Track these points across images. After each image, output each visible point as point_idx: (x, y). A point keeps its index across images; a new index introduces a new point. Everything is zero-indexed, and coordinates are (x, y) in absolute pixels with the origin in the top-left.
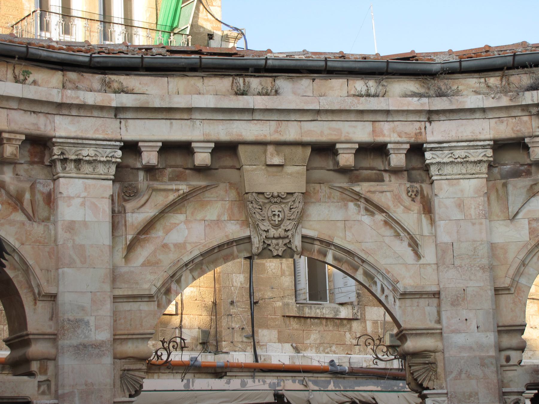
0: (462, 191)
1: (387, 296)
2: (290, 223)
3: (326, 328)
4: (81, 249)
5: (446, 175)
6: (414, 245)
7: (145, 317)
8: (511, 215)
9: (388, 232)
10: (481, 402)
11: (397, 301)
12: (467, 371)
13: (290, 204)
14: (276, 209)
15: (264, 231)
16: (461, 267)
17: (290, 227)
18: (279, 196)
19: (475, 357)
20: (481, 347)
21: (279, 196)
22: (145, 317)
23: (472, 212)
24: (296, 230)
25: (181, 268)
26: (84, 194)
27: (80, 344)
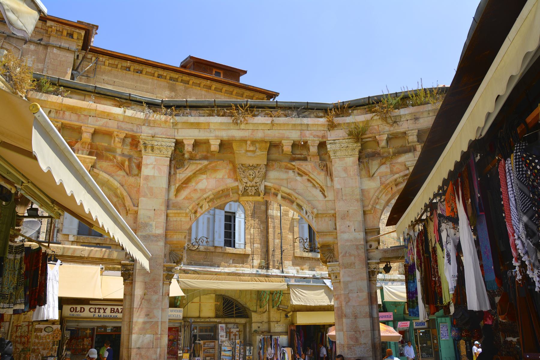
0: (346, 163)
1: (308, 216)
3: (312, 262)
4: (151, 189)
5: (338, 156)
6: (322, 191)
7: (184, 224)
8: (371, 175)
9: (310, 185)
10: (356, 267)
11: (314, 218)
13: (258, 170)
14: (251, 172)
17: (258, 181)
18: (253, 166)
19: (353, 245)
21: (253, 166)
22: (184, 224)
23: (351, 173)
25: (202, 200)
26: (154, 163)
27: (147, 235)
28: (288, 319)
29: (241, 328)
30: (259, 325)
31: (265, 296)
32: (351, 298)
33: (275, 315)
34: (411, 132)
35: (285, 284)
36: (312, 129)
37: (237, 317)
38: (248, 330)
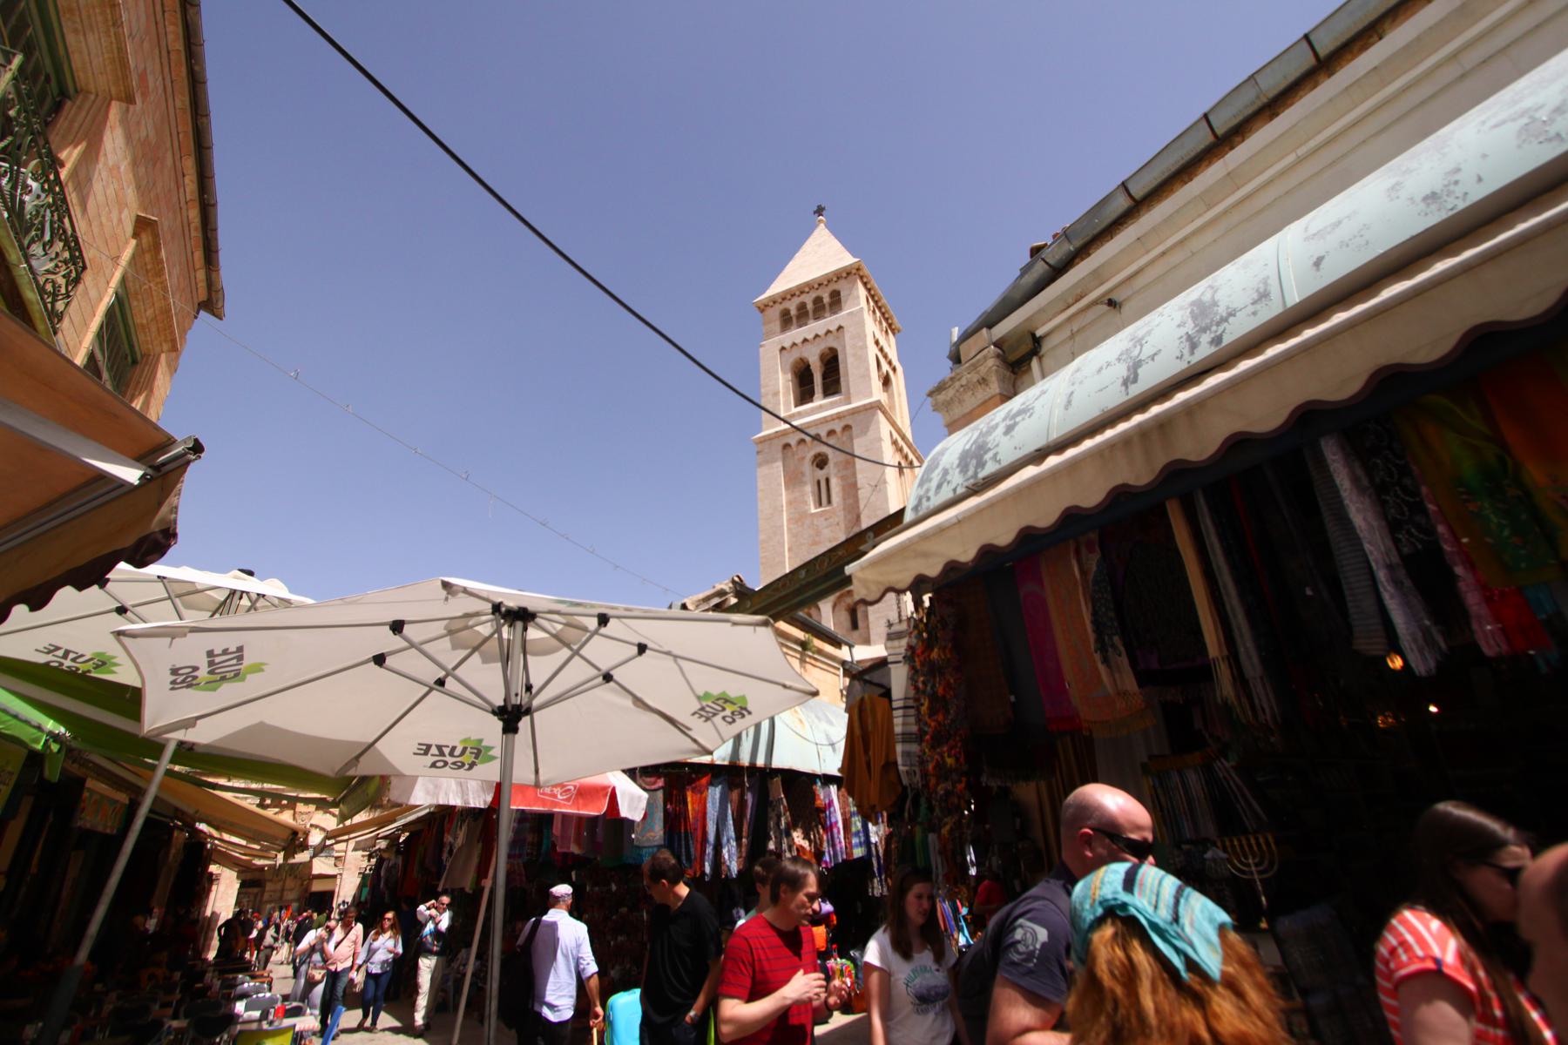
29: (252, 898)
30: (272, 894)
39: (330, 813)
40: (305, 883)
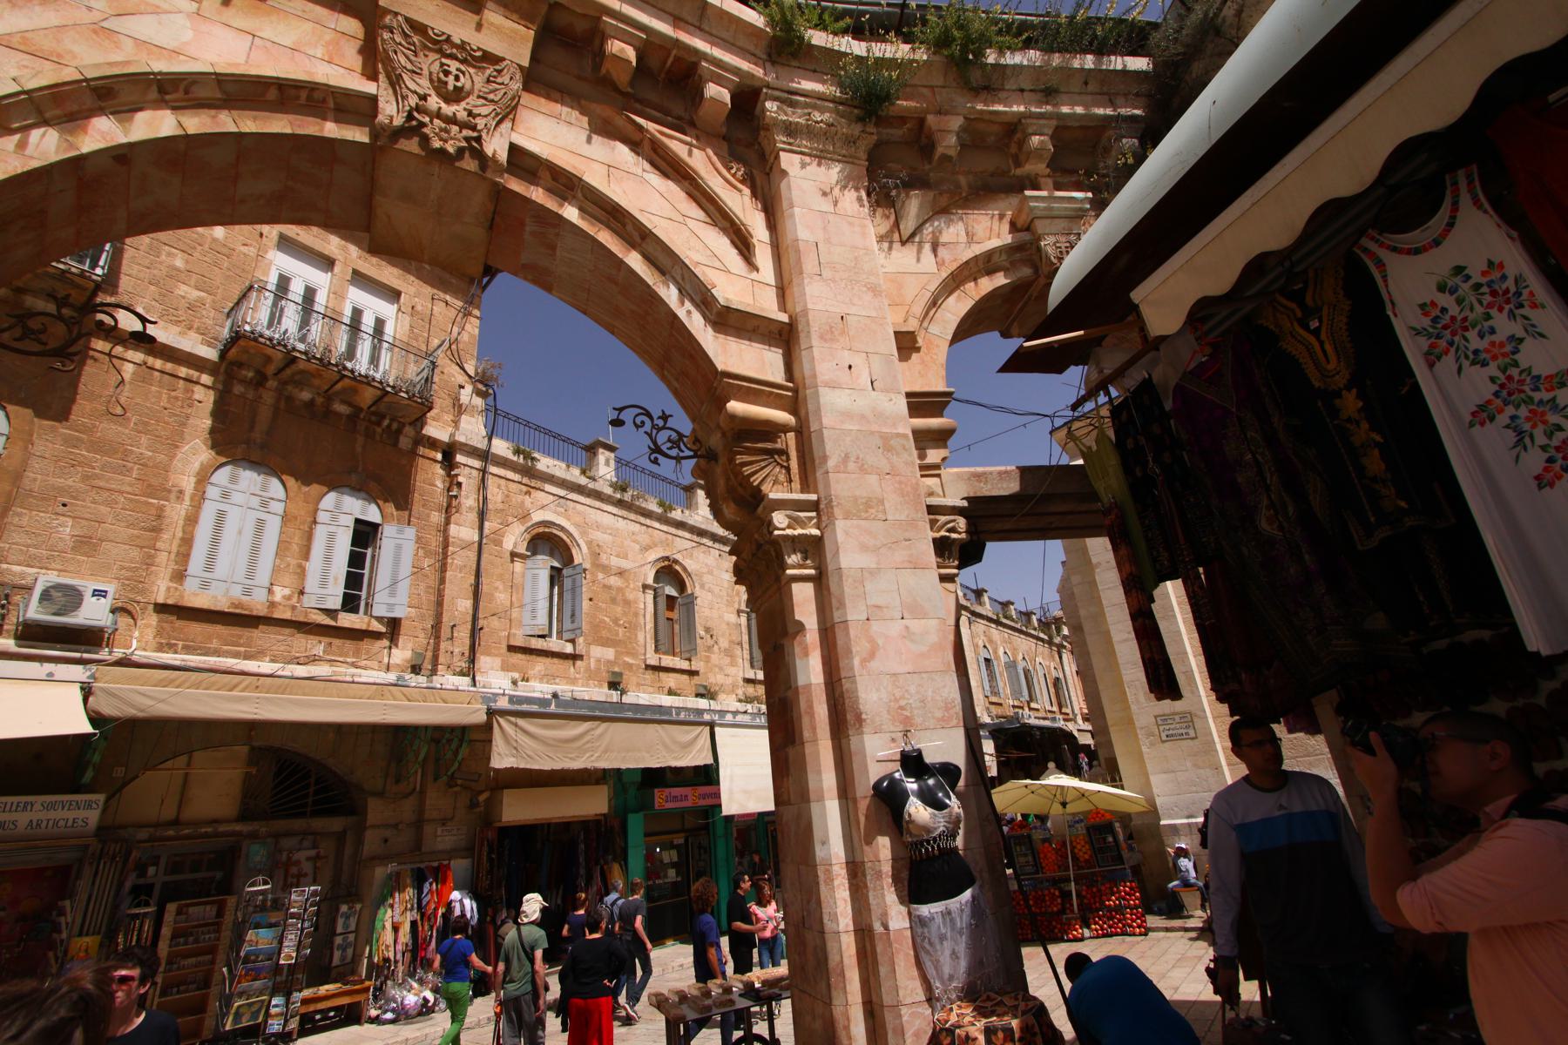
2: (486, 105)
12: (858, 458)
13: (488, 72)
14: (454, 66)
15: (415, 92)
16: (834, 281)
17: (484, 111)
19: (872, 433)
20: (879, 415)
24: (497, 125)
28: (478, 810)
30: (388, 833)
31: (415, 748)
32: (880, 642)
33: (437, 801)
34: (1035, 121)
35: (479, 710)
36: (714, 32)
37: (316, 813)
38: (348, 851)
39: (638, 143)
40: (482, 798)
